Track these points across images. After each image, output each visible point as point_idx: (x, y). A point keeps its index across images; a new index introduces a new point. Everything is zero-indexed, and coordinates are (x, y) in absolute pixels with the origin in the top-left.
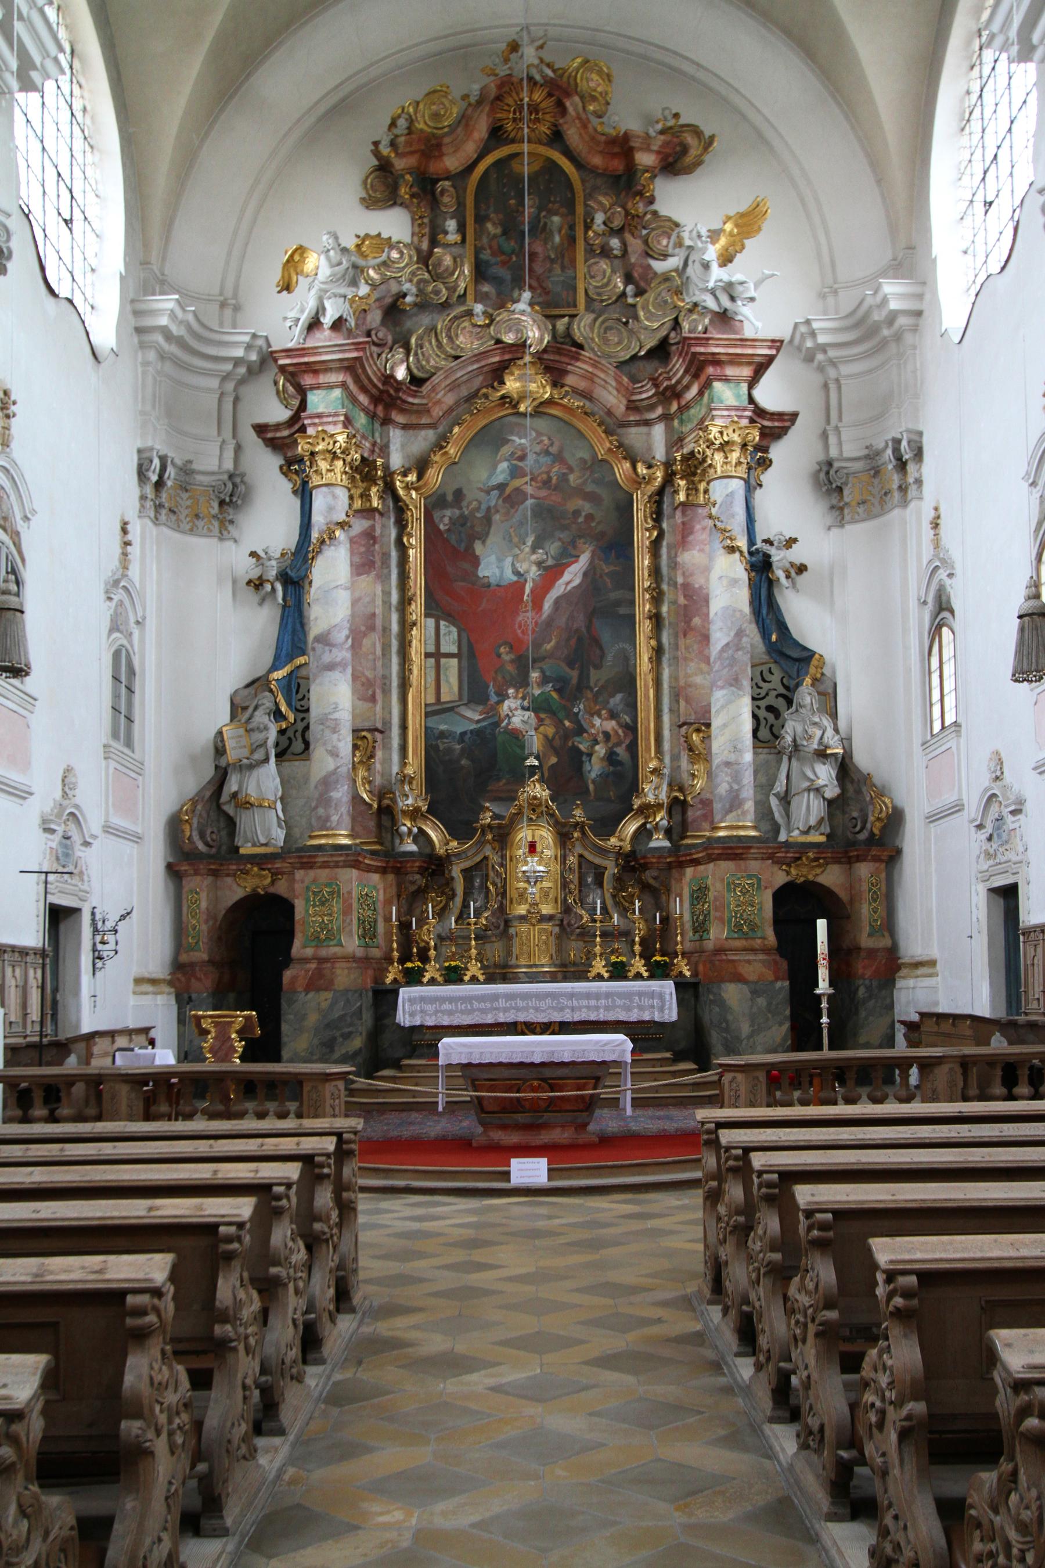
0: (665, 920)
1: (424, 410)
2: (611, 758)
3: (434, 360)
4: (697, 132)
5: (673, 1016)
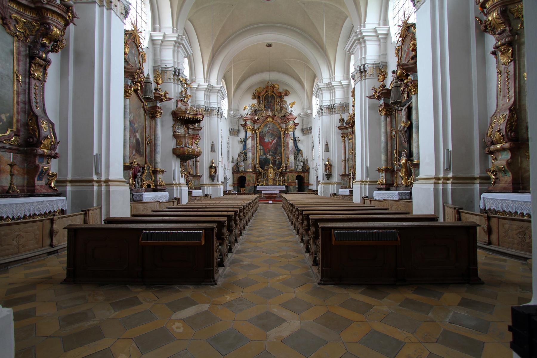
0: (285, 179)
1: (259, 122)
2: (279, 161)
3: (260, 117)
4: (288, 91)
5: (285, 189)
